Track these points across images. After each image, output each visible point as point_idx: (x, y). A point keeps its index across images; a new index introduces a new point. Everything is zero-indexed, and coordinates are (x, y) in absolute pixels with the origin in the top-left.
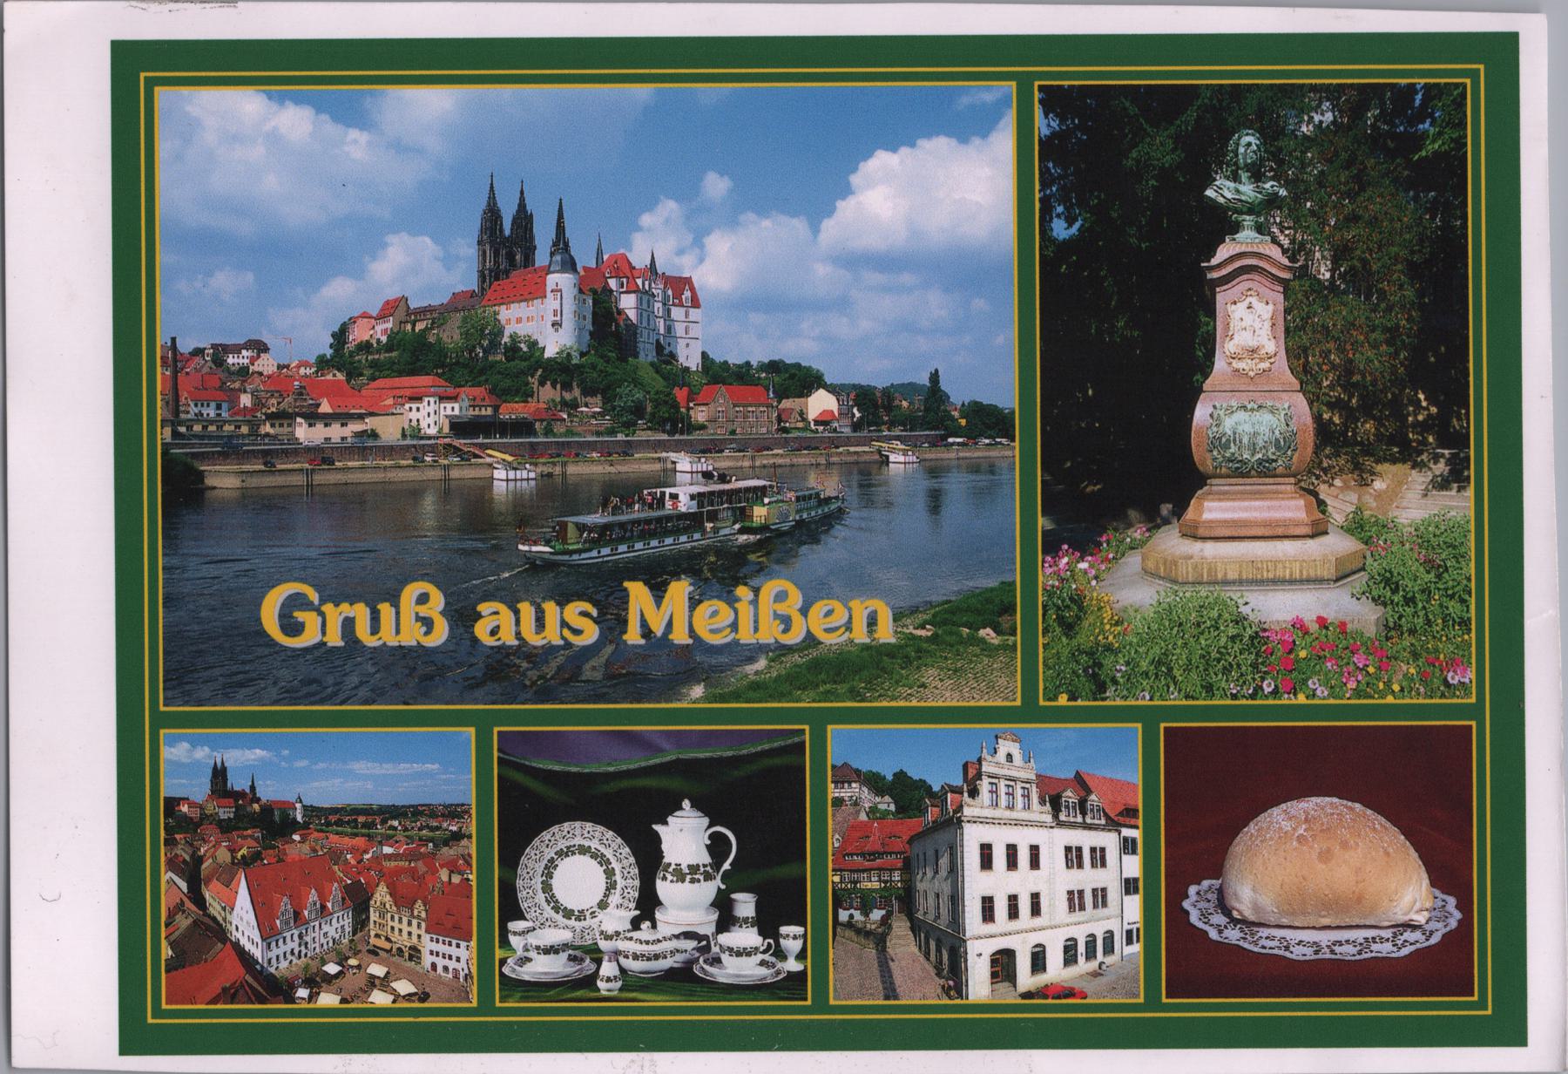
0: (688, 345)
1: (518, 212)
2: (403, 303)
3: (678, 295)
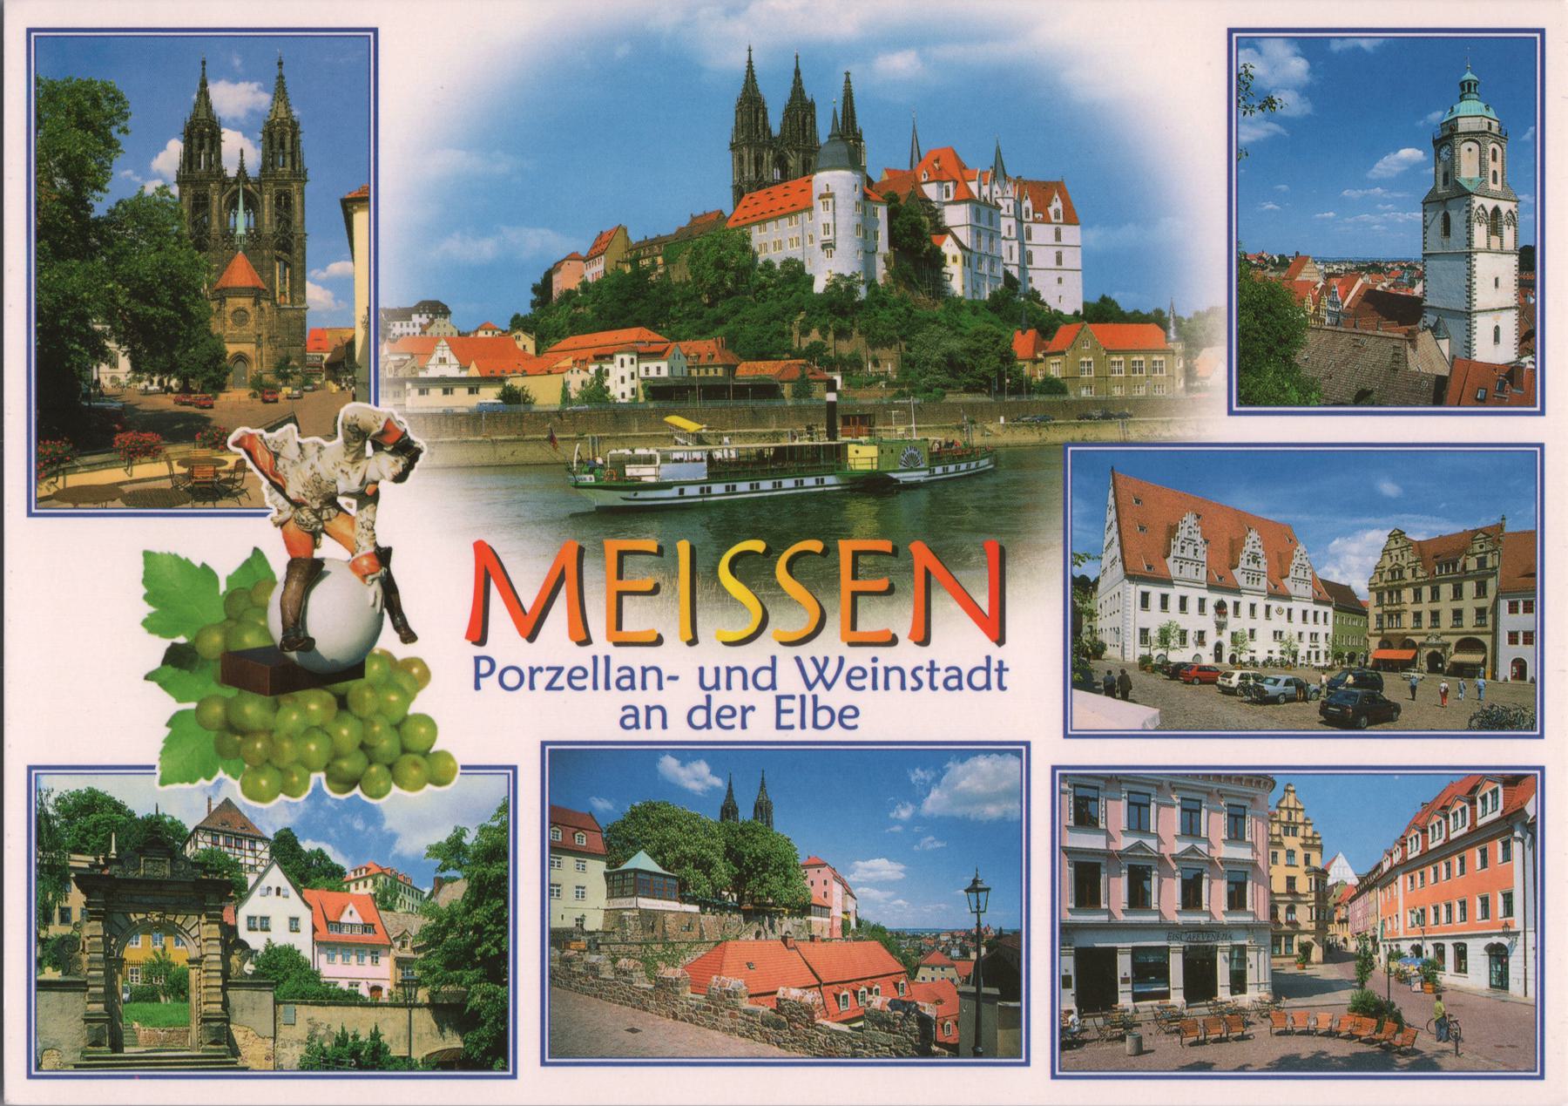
0: (1060, 280)
3: (1041, 206)
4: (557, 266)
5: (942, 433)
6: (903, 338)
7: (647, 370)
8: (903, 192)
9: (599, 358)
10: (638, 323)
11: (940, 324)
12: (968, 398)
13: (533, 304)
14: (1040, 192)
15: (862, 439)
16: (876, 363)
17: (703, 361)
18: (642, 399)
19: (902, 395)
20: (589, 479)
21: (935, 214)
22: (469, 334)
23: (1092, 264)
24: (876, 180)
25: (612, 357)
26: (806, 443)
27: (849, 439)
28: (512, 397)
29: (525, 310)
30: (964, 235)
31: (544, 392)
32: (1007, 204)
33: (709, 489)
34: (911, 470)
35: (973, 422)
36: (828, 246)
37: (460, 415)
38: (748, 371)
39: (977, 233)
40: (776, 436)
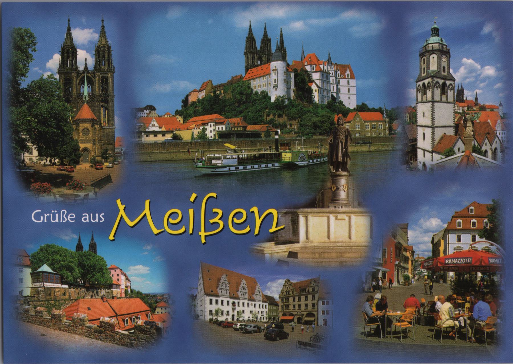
0: (349, 98)
1: (264, 38)
2: (210, 82)
3: (343, 73)
4: (190, 94)
5: (312, 148)
6: (299, 117)
7: (219, 128)
8: (299, 68)
9: (203, 124)
10: (215, 113)
11: (311, 113)
12: (320, 137)
13: (182, 106)
14: (343, 68)
15: (287, 151)
16: (291, 126)
17: (236, 125)
18: (217, 138)
19: (299, 136)
20: (200, 164)
21: (309, 76)
22: (162, 116)
23: (359, 92)
24: (290, 64)
25: (207, 124)
26: (269, 152)
27: (282, 151)
28: (176, 137)
29: (180, 108)
30: (319, 83)
31: (186, 136)
32: (332, 72)
33: (238, 168)
34: (302, 161)
35: (322, 145)
36: (275, 87)
37: (159, 143)
38: (250, 128)
39: (323, 81)
40: (259, 150)
